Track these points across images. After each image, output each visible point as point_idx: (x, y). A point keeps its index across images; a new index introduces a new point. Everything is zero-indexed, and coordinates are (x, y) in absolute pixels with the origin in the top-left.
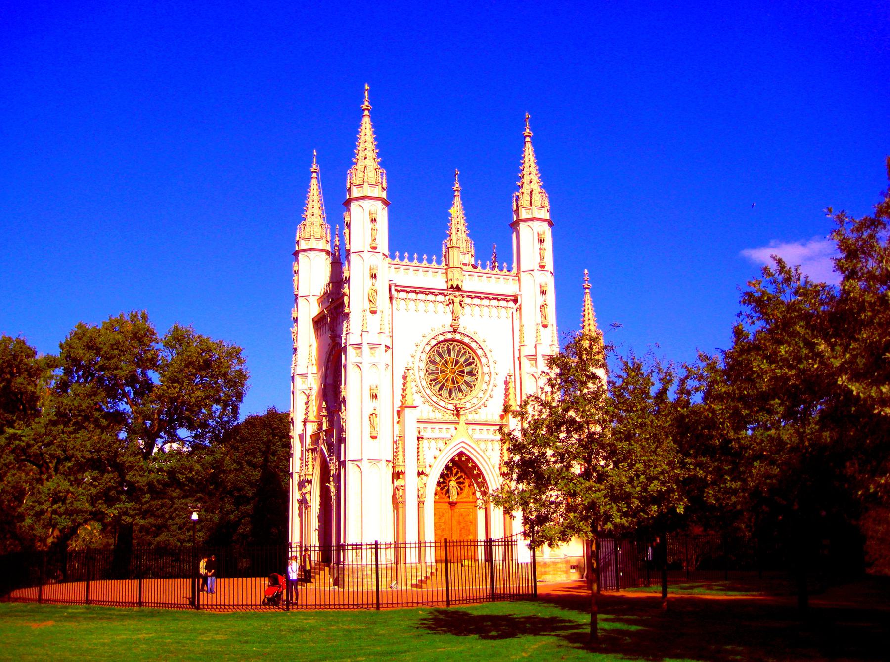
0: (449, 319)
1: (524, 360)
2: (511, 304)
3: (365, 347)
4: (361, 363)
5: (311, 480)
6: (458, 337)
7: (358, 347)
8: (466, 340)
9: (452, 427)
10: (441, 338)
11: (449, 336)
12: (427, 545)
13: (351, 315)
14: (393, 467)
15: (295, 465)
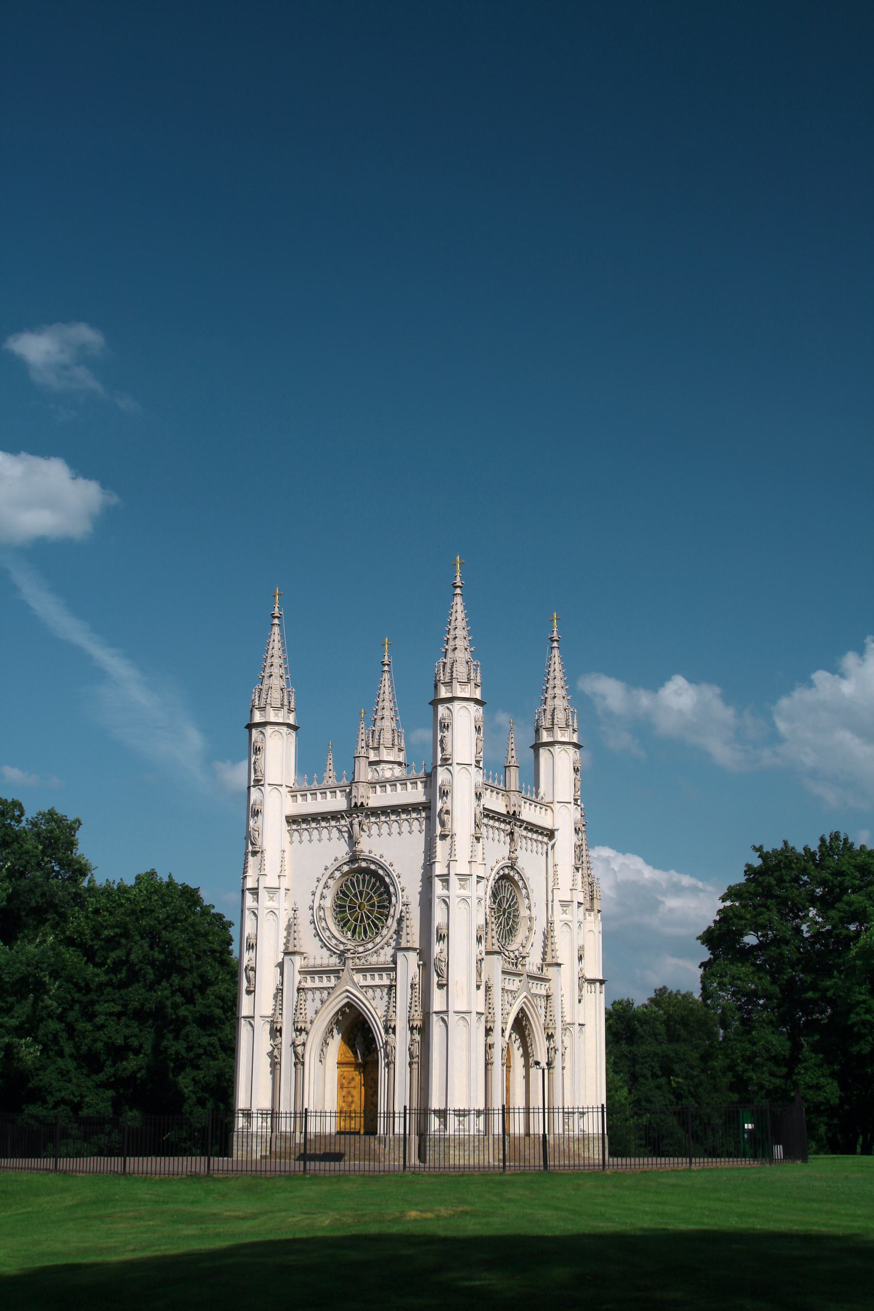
0: (505, 851)
1: (557, 904)
2: (546, 839)
3: (453, 880)
4: (469, 897)
5: (281, 1029)
6: (512, 874)
7: (463, 878)
8: (516, 877)
9: (517, 979)
10: (501, 873)
11: (506, 871)
12: (496, 1112)
13: (456, 838)
14: (487, 1022)
15: (257, 1004)
